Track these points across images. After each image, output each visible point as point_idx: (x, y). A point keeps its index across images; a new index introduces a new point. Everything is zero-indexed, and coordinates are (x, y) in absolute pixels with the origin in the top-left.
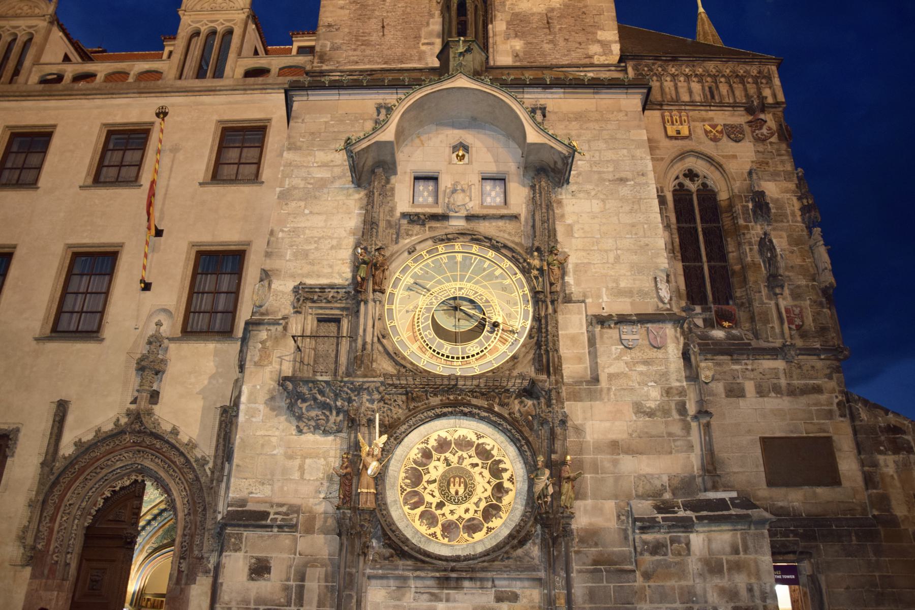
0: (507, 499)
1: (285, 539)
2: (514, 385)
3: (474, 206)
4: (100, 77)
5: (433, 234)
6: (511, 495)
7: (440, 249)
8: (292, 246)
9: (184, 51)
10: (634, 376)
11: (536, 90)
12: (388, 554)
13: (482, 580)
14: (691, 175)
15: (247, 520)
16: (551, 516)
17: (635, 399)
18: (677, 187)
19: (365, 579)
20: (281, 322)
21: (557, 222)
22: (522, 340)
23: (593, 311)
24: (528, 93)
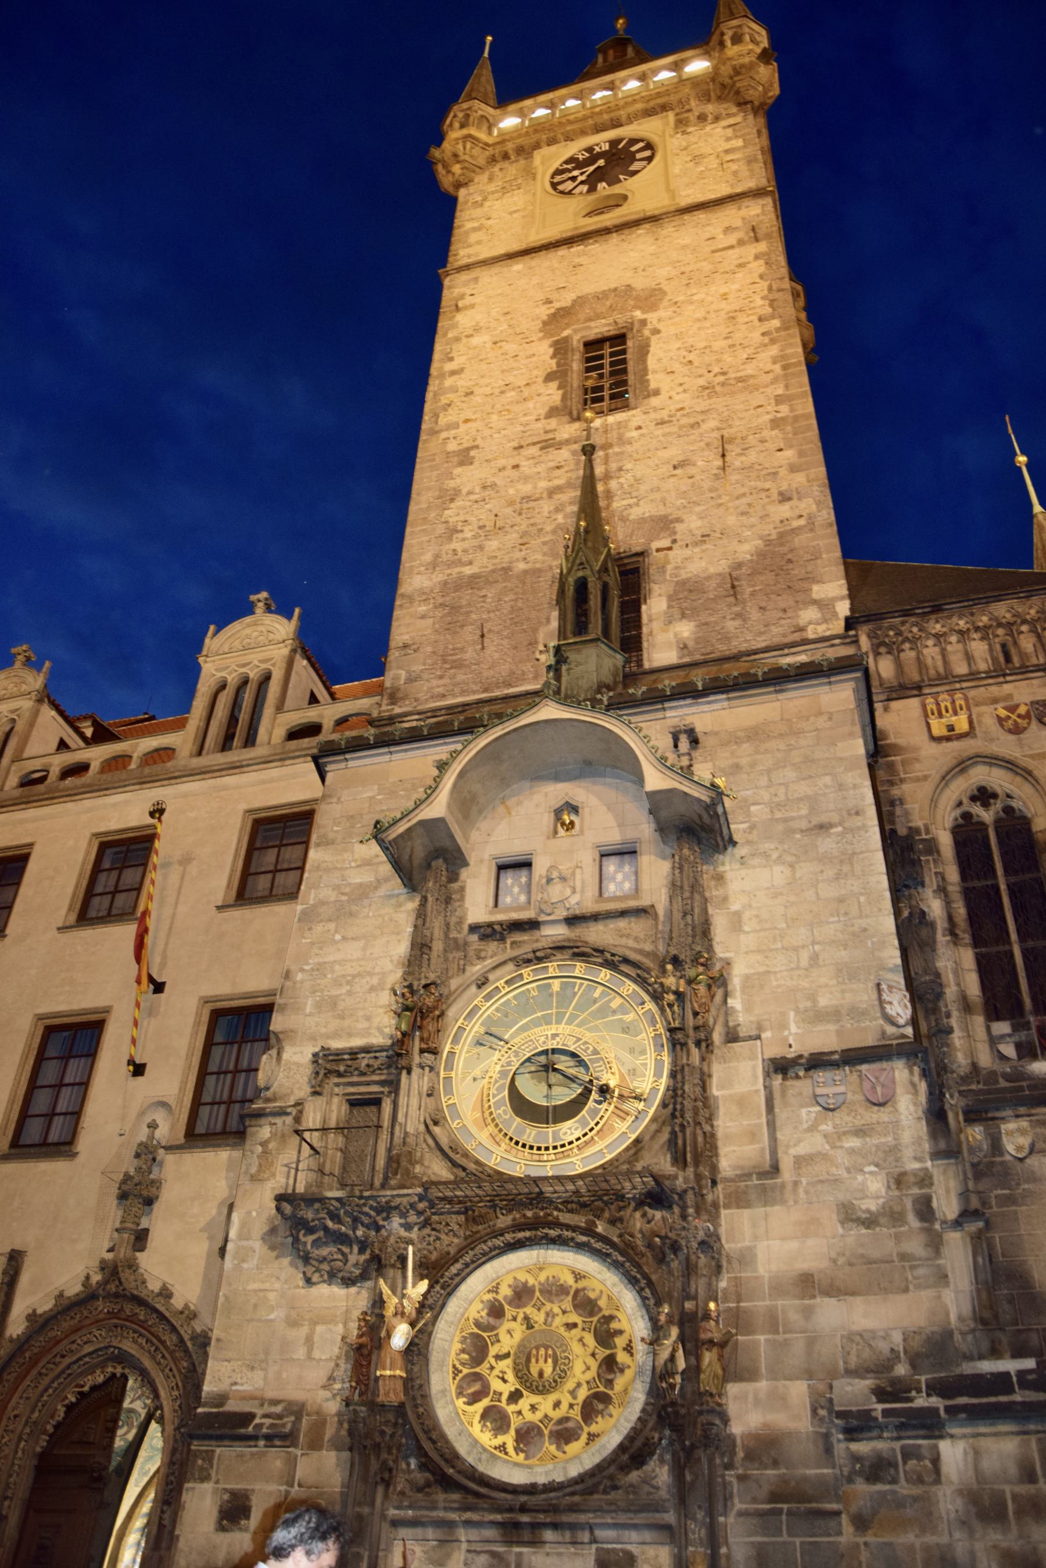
1: (275, 1459)
2: (633, 1187)
3: (584, 900)
4: (95, 766)
6: (629, 1373)
8: (314, 992)
9: (204, 714)
10: (841, 1157)
11: (682, 702)
12: (422, 1482)
13: (573, 1527)
14: (983, 796)
15: (219, 1428)
16: (683, 1411)
17: (841, 1196)
19: (385, 1526)
20: (289, 1110)
21: (710, 911)
22: (651, 1112)
23: (775, 1051)
24: (671, 708)
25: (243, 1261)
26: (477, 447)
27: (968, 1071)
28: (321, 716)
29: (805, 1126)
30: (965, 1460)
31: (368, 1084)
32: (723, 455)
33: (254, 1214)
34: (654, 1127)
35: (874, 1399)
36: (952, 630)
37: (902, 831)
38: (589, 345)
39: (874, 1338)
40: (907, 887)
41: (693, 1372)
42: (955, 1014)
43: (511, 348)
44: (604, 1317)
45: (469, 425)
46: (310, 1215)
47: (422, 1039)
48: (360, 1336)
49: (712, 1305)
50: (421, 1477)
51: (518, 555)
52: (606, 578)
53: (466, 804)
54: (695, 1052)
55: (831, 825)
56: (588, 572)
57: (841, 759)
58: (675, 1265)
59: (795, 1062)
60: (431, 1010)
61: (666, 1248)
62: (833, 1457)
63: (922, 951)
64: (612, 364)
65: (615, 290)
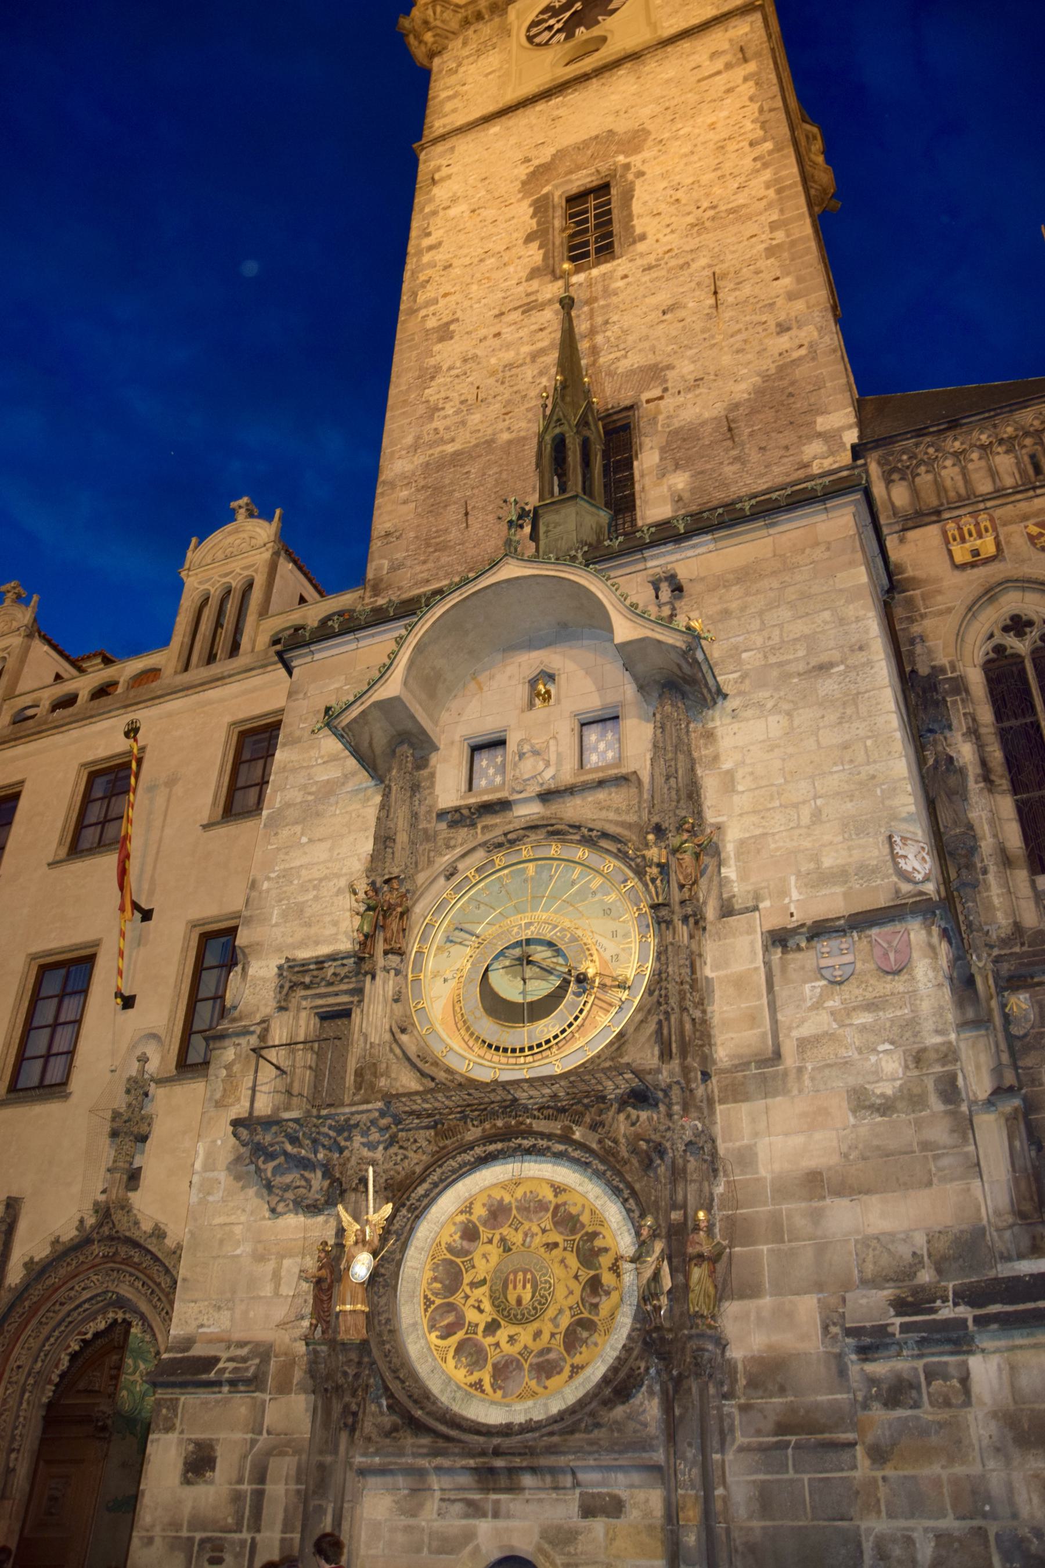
0: (606, 1305)
1: (240, 1405)
2: (614, 1087)
4: (83, 696)
5: (488, 836)
6: (615, 1296)
7: (497, 862)
9: (189, 630)
10: (851, 1036)
11: (663, 549)
12: (388, 1427)
13: (553, 1471)
14: (1017, 625)
15: (182, 1374)
17: (852, 1081)
18: (992, 655)
19: (350, 1476)
21: (699, 772)
23: (775, 922)
24: (653, 557)
25: (209, 1194)
26: (457, 320)
27: (1009, 932)
28: (304, 617)
29: (809, 1004)
30: (1000, 1378)
32: (715, 293)
33: (219, 1142)
35: (892, 1312)
36: (972, 446)
37: (923, 670)
38: (571, 200)
39: (893, 1242)
40: (931, 731)
41: (680, 1292)
42: (992, 869)
43: (489, 213)
44: (587, 1233)
45: (448, 299)
47: (385, 940)
48: (320, 1269)
49: (701, 1215)
50: (388, 1420)
51: (501, 425)
52: (587, 433)
53: (430, 682)
54: (683, 931)
55: (832, 665)
56: (566, 428)
57: (841, 590)
58: (662, 1170)
59: (794, 931)
60: (391, 907)
62: (848, 1380)
63: (951, 801)
64: (597, 217)
65: (597, 137)
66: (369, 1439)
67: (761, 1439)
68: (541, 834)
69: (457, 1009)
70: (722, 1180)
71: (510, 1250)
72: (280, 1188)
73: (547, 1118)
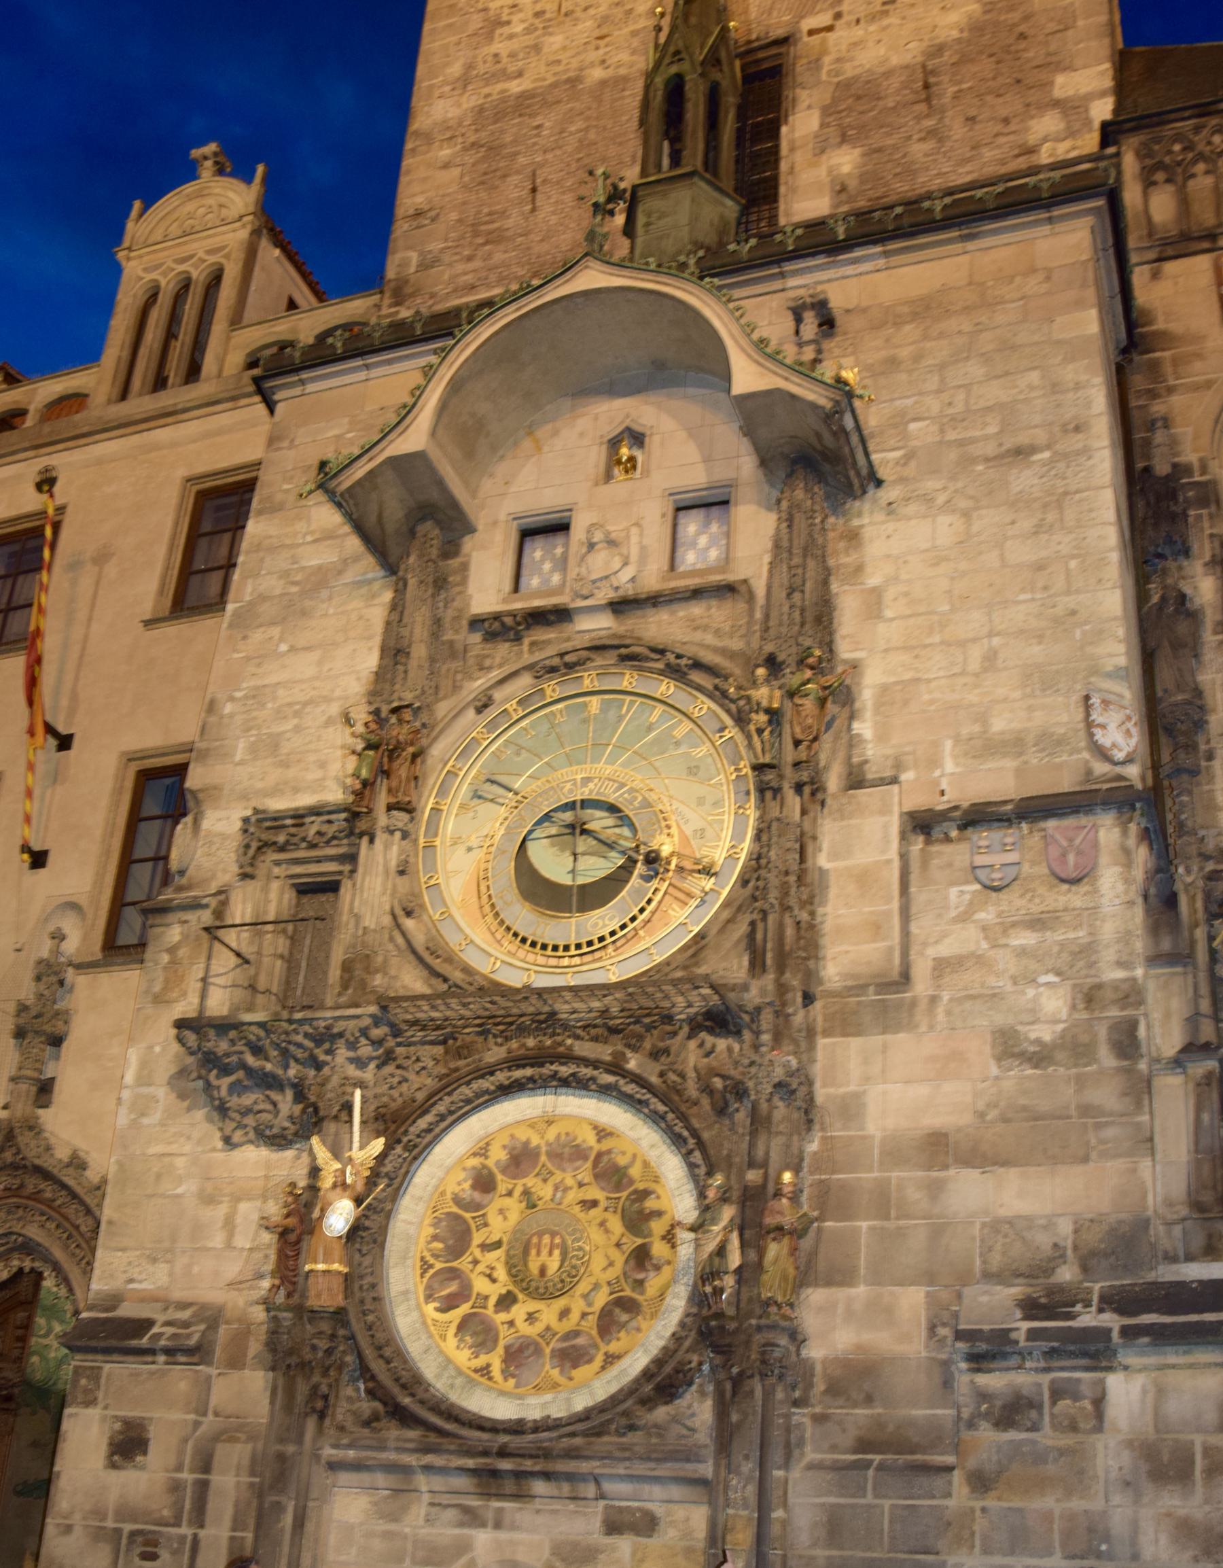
0: (654, 1283)
1: (180, 1379)
2: (686, 1004)
5: (538, 656)
6: (666, 1270)
7: (548, 692)
15: (105, 1338)
16: (732, 1326)
21: (835, 587)
23: (919, 801)
24: (795, 273)
25: (143, 1115)
29: (953, 913)
31: (318, 861)
33: (157, 1049)
34: (726, 914)
41: (748, 1273)
44: (636, 1192)
46: (223, 1046)
47: (390, 791)
48: (288, 1216)
49: (787, 1177)
50: (367, 1406)
54: (794, 803)
59: (943, 816)
61: (729, 1094)
66: (342, 1429)
67: (836, 1456)
68: (610, 658)
69: (483, 889)
70: (817, 1135)
71: (534, 1206)
72: (238, 1111)
73: (595, 1039)
